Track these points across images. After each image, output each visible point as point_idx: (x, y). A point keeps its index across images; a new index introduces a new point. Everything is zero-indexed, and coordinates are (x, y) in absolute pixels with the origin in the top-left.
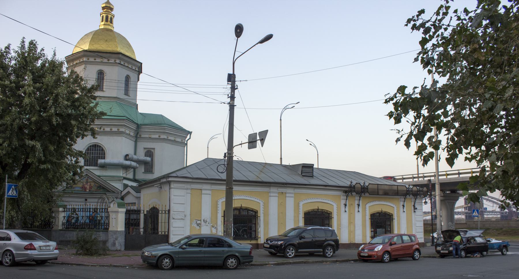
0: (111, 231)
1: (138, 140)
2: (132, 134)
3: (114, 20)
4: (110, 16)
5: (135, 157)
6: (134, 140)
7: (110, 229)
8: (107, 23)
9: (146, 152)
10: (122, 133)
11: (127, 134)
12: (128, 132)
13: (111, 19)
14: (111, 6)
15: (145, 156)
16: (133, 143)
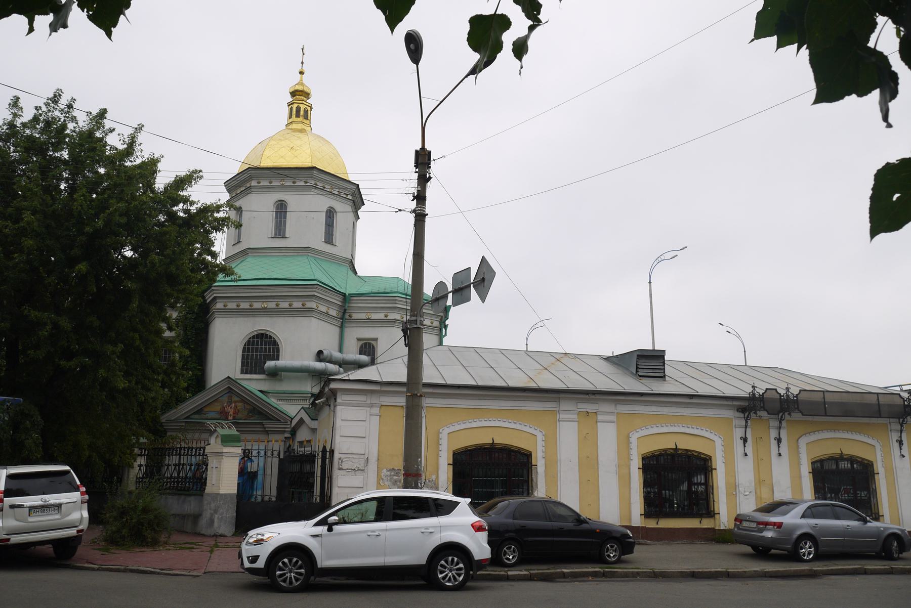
0: (208, 494)
1: (347, 324)
2: (333, 313)
3: (313, 114)
4: (302, 107)
5: (337, 355)
6: (339, 324)
7: (208, 490)
8: (298, 119)
9: (361, 347)
10: (310, 310)
11: (321, 313)
12: (323, 309)
13: (306, 112)
14: (306, 90)
15: (361, 353)
16: (337, 330)
